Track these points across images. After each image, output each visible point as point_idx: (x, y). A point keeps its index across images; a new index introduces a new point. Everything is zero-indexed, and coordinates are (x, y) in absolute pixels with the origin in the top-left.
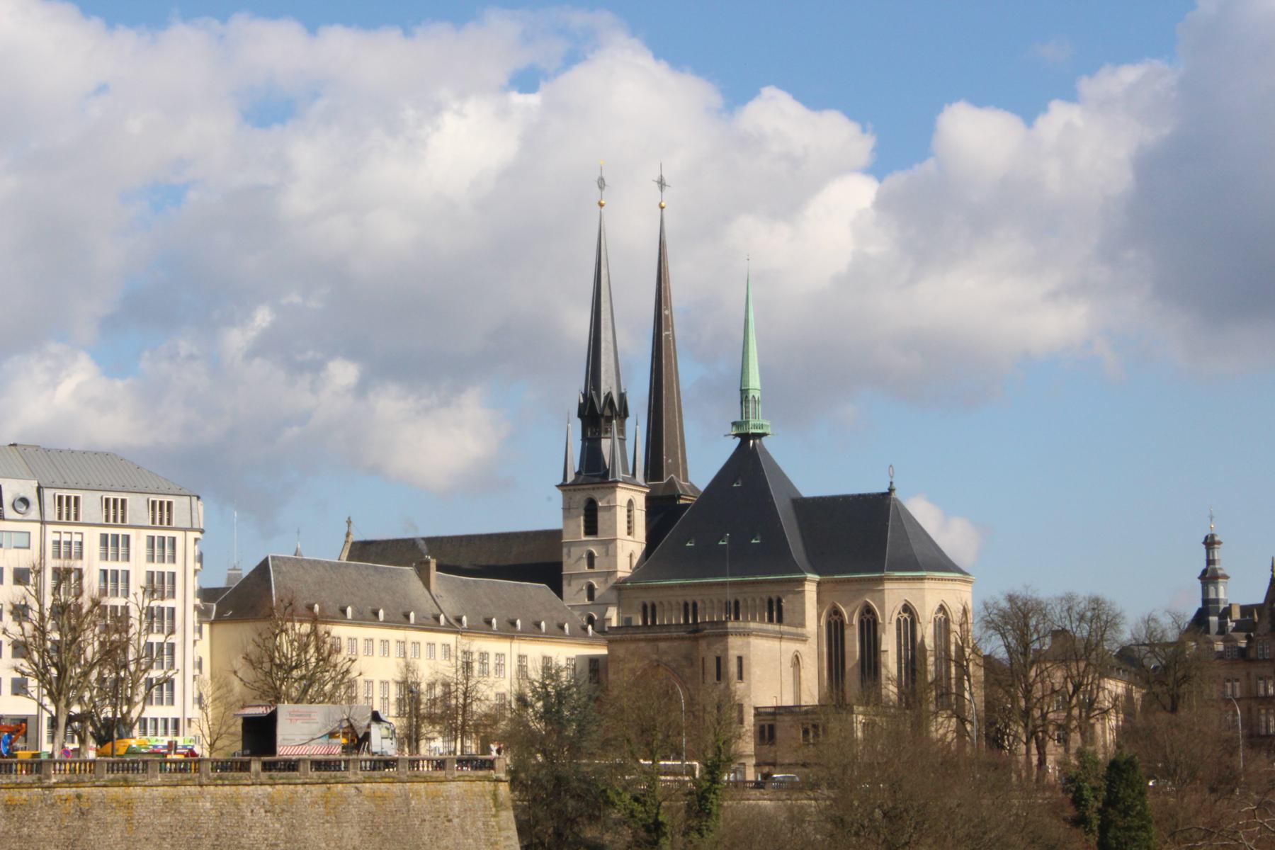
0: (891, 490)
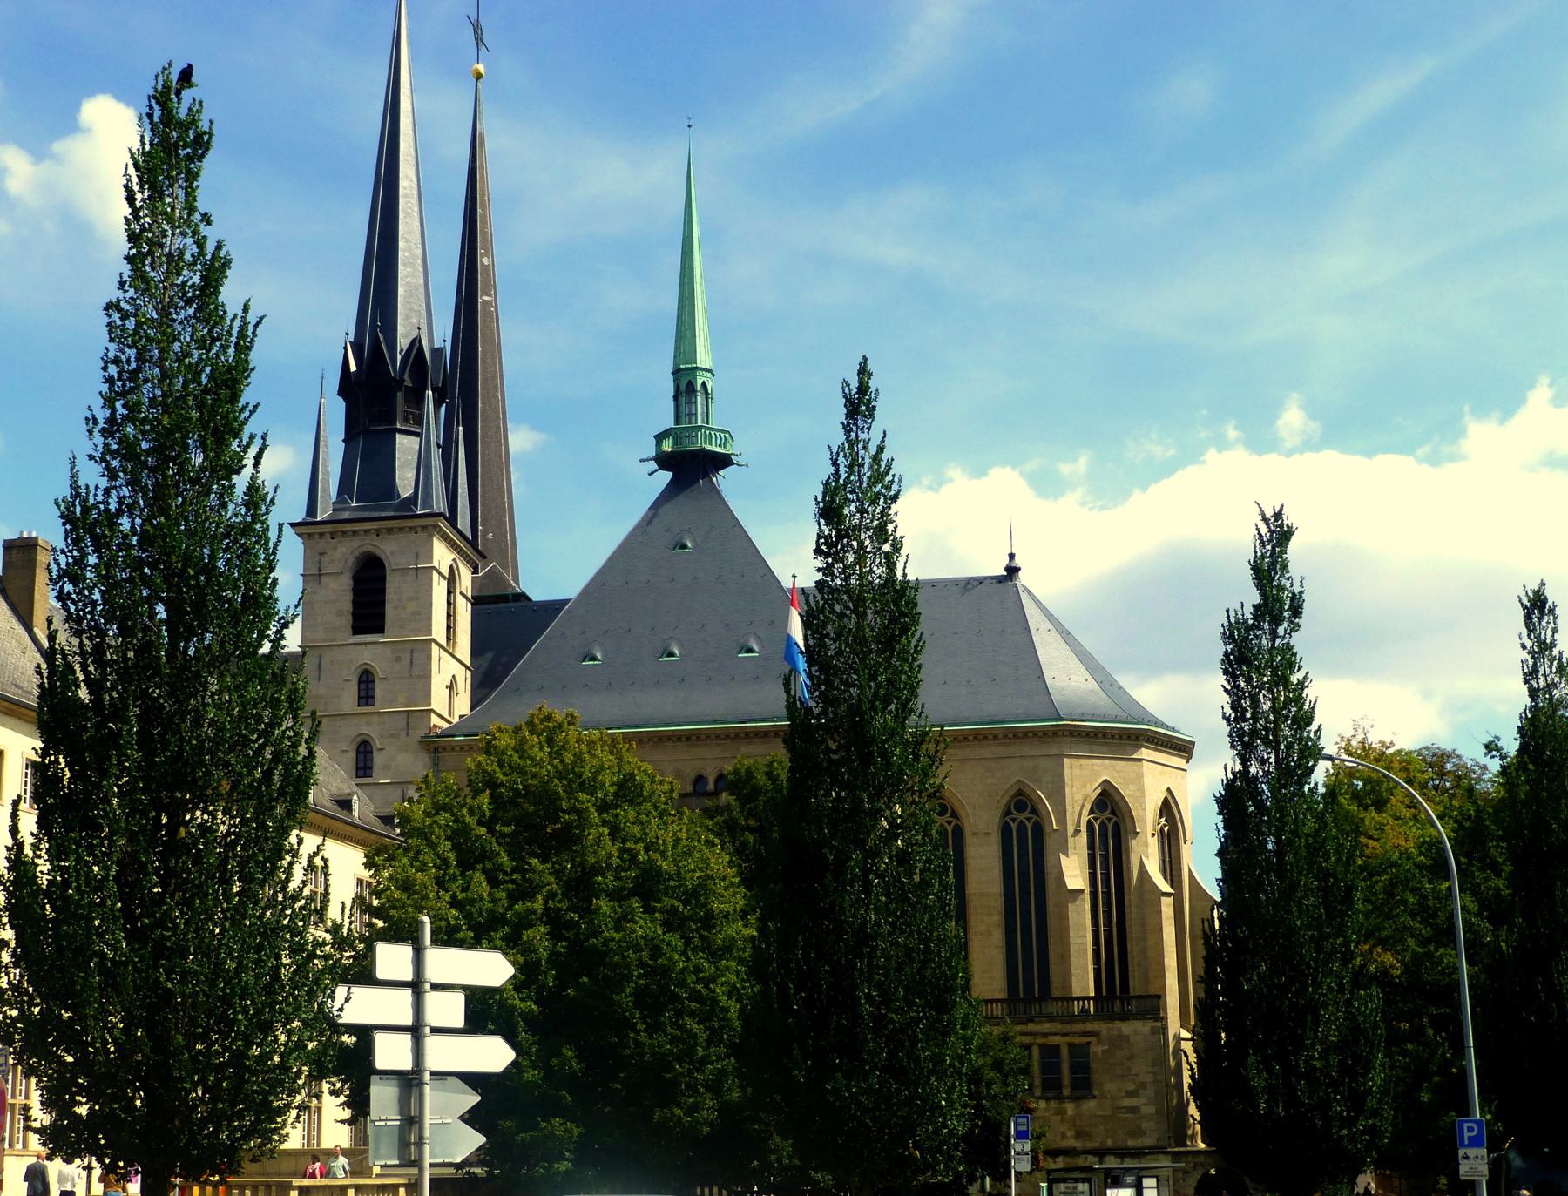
0: (1012, 571)
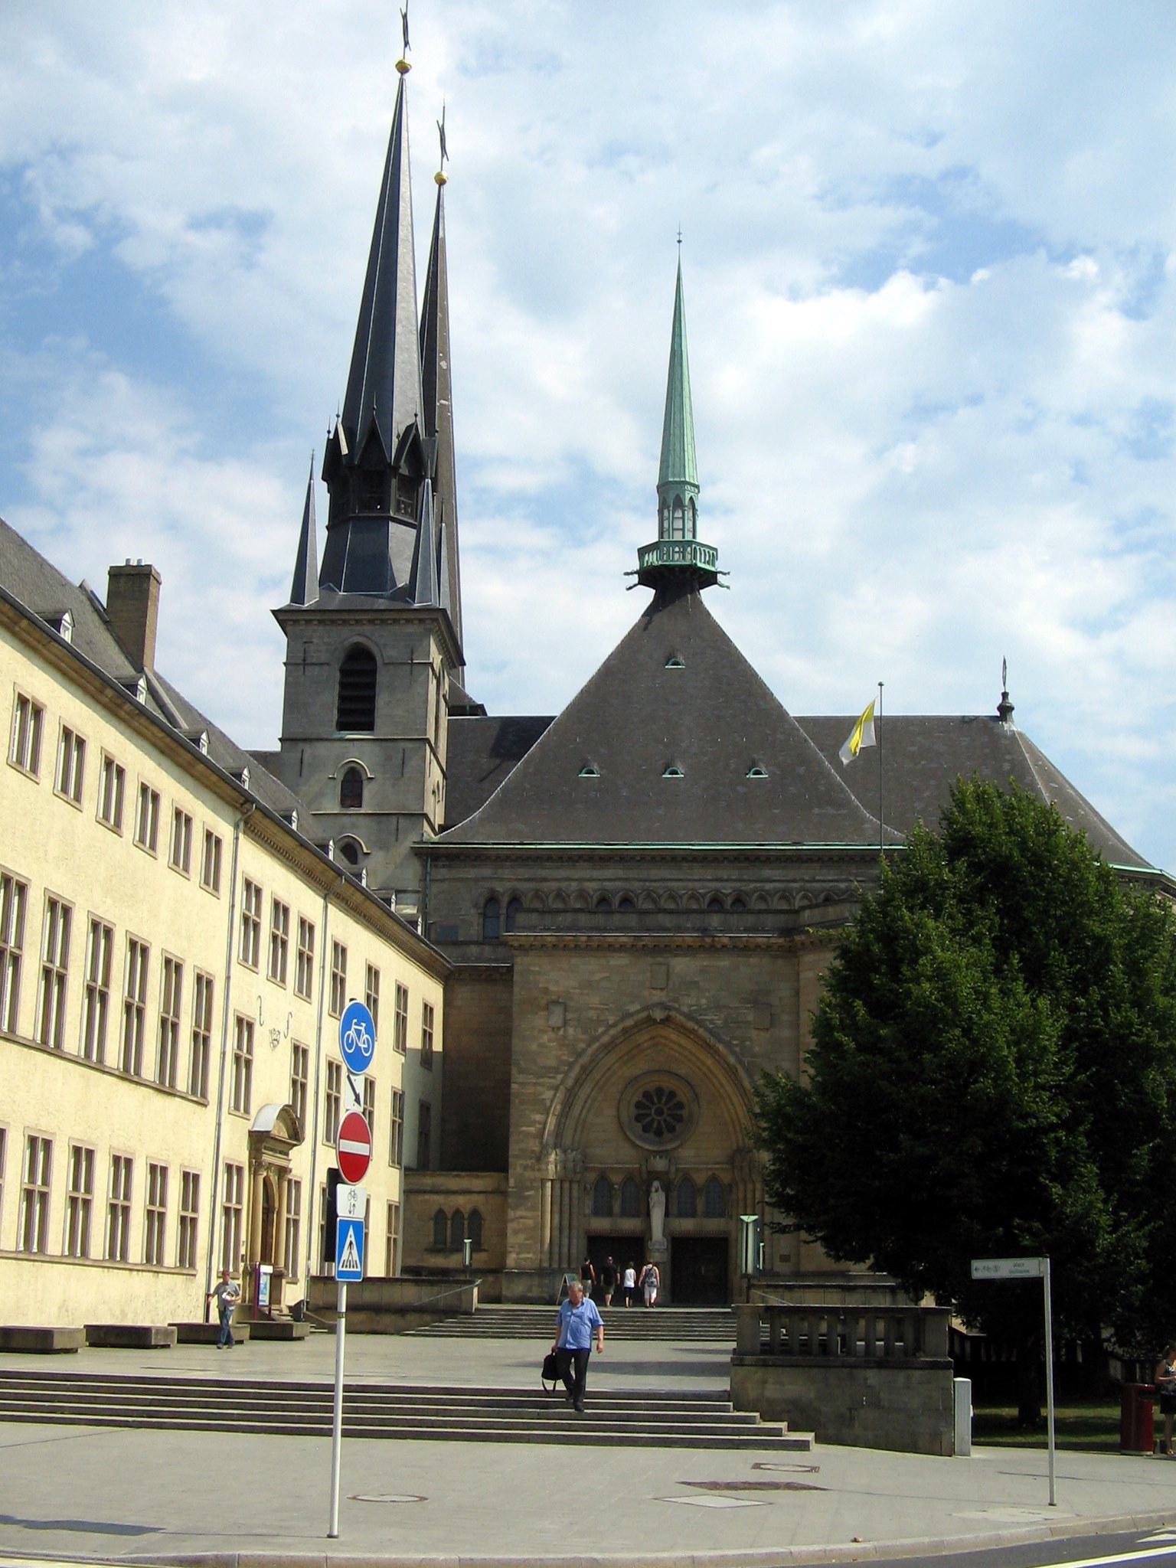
0: (1005, 710)
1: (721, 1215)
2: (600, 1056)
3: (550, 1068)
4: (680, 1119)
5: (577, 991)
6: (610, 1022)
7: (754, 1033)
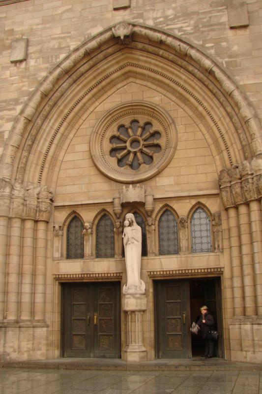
1: (213, 248)
2: (65, 85)
3: (10, 100)
4: (158, 146)
5: (40, 26)
6: (72, 48)
7: (230, 33)
